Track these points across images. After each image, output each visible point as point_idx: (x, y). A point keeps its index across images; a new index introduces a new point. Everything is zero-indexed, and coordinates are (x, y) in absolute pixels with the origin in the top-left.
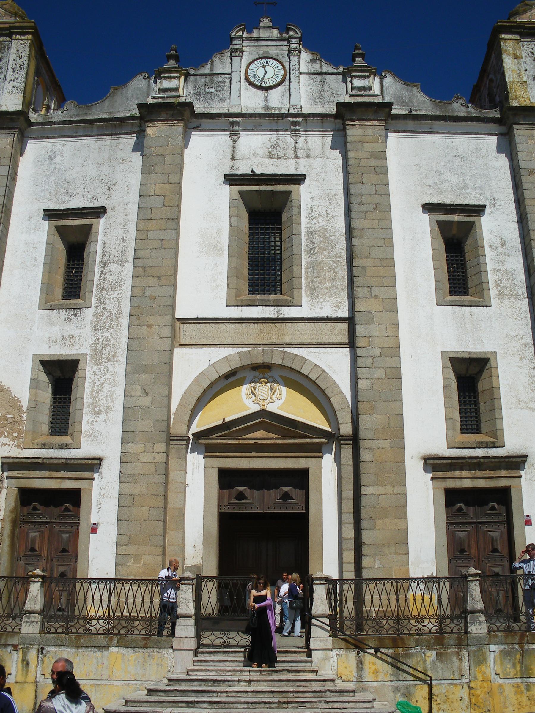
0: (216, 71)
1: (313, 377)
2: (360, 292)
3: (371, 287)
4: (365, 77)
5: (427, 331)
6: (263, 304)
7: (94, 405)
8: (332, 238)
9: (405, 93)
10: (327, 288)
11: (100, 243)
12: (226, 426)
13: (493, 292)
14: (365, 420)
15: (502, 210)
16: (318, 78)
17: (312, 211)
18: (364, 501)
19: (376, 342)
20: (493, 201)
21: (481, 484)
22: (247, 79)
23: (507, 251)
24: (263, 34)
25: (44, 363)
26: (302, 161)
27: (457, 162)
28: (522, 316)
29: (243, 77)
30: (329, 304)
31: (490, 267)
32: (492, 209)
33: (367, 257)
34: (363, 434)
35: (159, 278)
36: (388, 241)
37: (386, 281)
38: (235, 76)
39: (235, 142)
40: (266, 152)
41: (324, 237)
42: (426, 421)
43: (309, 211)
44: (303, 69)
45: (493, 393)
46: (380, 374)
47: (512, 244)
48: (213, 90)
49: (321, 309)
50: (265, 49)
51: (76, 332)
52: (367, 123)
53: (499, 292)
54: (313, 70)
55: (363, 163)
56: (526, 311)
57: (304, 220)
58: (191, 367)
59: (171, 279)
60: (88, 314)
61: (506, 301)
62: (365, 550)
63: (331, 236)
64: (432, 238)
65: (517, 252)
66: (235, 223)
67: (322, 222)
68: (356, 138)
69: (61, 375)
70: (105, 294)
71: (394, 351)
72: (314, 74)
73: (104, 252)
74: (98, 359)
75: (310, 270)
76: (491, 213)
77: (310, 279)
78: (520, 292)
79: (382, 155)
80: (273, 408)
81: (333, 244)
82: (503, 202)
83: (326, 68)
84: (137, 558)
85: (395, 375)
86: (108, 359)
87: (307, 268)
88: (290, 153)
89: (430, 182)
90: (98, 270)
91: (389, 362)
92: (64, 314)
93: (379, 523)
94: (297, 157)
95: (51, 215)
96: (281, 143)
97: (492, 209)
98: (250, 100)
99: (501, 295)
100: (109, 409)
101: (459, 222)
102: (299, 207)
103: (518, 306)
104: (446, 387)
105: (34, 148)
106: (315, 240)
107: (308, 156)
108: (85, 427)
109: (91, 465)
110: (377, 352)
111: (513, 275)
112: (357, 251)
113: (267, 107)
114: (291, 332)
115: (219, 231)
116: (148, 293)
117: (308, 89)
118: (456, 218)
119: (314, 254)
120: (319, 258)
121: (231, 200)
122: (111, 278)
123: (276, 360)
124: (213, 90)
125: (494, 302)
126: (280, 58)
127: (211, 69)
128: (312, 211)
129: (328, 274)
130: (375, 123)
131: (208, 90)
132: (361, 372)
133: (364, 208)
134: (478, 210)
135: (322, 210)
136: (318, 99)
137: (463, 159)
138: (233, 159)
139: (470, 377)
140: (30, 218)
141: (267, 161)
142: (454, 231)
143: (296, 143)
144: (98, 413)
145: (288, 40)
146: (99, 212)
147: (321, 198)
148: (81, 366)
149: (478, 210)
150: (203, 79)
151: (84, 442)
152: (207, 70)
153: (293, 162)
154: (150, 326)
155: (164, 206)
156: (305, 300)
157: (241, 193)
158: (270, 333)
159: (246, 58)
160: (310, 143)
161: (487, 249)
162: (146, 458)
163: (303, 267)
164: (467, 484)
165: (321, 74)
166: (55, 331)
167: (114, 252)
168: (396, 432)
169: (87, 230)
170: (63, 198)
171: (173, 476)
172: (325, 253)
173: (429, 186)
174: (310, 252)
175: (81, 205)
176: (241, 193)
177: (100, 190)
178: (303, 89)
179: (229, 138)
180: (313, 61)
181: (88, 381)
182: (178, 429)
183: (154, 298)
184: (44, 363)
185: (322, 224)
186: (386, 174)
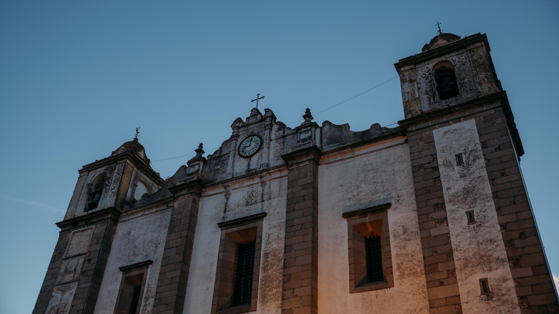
0: (223, 154)
3: (293, 289)
4: (308, 131)
8: (280, 255)
9: (337, 134)
10: (273, 294)
13: (396, 274)
15: (404, 204)
16: (281, 140)
17: (269, 238)
20: (397, 198)
22: (239, 154)
23: (407, 237)
26: (265, 203)
27: (371, 174)
28: (420, 290)
29: (237, 153)
30: (273, 306)
31: (393, 254)
32: (397, 205)
33: (293, 267)
35: (167, 305)
38: (231, 155)
39: (227, 199)
40: (245, 201)
41: (274, 255)
43: (267, 238)
44: (273, 136)
47: (412, 230)
48: (219, 167)
49: (268, 311)
52: (301, 165)
53: (401, 273)
54: (279, 135)
56: (423, 286)
57: (263, 245)
61: (406, 280)
63: (279, 254)
64: (349, 239)
65: (417, 236)
66: (221, 258)
67: (274, 245)
72: (279, 139)
73: (148, 290)
75: (264, 282)
76: (396, 208)
77: (263, 290)
78: (418, 270)
82: (405, 197)
87: (262, 281)
88: (260, 198)
89: (349, 196)
90: (143, 303)
95: (124, 269)
96: (254, 193)
97: (397, 205)
99: (402, 275)
102: (261, 237)
103: (417, 282)
105: (121, 229)
106: (269, 259)
111: (412, 256)
115: (212, 264)
117: (275, 150)
119: (267, 270)
120: (270, 272)
121: (221, 241)
125: (396, 283)
127: (220, 153)
128: (269, 238)
129: (275, 283)
130: (307, 163)
131: (216, 168)
133: (294, 229)
135: (274, 236)
137: (375, 170)
138: (225, 211)
141: (244, 208)
143: (263, 191)
147: (275, 227)
155: (177, 254)
156: (259, 305)
159: (240, 140)
160: (272, 188)
161: (392, 239)
163: (260, 281)
170: (132, 258)
172: (274, 268)
173: (349, 199)
174: (265, 270)
175: (141, 261)
176: (227, 234)
177: (151, 249)
178: (272, 151)
179: (224, 198)
185: (274, 246)
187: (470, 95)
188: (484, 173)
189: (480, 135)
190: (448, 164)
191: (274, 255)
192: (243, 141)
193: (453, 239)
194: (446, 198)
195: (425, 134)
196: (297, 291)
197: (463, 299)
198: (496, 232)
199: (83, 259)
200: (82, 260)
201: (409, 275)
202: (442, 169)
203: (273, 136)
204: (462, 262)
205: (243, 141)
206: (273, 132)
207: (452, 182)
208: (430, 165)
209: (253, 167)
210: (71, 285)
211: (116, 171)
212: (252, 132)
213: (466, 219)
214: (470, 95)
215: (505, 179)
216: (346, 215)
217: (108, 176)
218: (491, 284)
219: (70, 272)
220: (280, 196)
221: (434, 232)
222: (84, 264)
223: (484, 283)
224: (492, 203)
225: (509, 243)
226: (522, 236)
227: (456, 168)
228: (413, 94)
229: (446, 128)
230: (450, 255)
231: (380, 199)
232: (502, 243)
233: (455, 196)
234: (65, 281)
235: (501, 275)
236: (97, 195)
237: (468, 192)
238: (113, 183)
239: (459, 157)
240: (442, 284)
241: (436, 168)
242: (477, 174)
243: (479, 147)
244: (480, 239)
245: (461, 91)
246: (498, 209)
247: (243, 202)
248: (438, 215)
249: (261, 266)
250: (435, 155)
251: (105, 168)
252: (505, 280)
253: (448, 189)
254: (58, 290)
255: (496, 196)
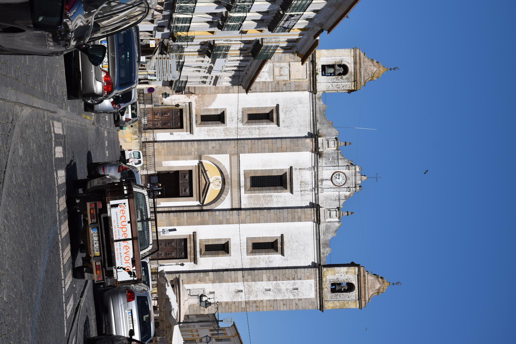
0: (340, 161)
1: (221, 198)
2: (248, 212)
5: (239, 234)
6: (245, 181)
7: (210, 130)
9: (332, 230)
11: (266, 126)
12: (205, 171)
13: (252, 257)
14: (206, 213)
18: (182, 213)
19: (231, 217)
21: (189, 250)
24: (358, 177)
25: (224, 112)
26: (300, 192)
34: (202, 213)
35: (251, 148)
36: (266, 221)
37: (252, 220)
39: (307, 169)
41: (270, 201)
42: (208, 232)
44: (341, 193)
45: (217, 255)
46: (221, 218)
48: (331, 160)
50: (351, 178)
51: (234, 122)
55: (296, 214)
57: (276, 194)
58: (224, 160)
59: (251, 151)
60: (241, 125)
61: (249, 261)
62: (167, 214)
67: (275, 200)
68: (306, 211)
69: (220, 118)
70: (248, 130)
71: (228, 222)
73: (263, 128)
74: (225, 130)
79: (300, 220)
80: (211, 186)
81: (267, 204)
83: (342, 202)
84: (163, 149)
85: (221, 223)
86: (225, 133)
88: (303, 189)
90: (256, 126)
91: (225, 221)
92: (240, 117)
93: (176, 218)
94: (301, 191)
95: (278, 106)
98: (326, 173)
99: (251, 259)
100: (209, 135)
101: (277, 247)
102: (281, 192)
104: (219, 239)
107: (301, 195)
108: (203, 128)
109: (191, 132)
110: (228, 217)
112: (262, 211)
113: (322, 180)
114: (235, 190)
116: (246, 146)
118: (279, 246)
120: (262, 199)
121: (283, 170)
122: (253, 131)
123: (226, 186)
124: (331, 160)
125: (249, 256)
126: (346, 184)
127: (341, 159)
130: (313, 218)
132: (221, 212)
133: (278, 214)
134: (282, 254)
135: (280, 200)
136: (327, 198)
138: (300, 169)
139: (223, 248)
140: (277, 99)
142: (276, 245)
144: (208, 132)
145: (355, 187)
146: (278, 124)
148: (223, 125)
149: (282, 254)
150: (336, 156)
151: (198, 128)
152: (340, 157)
153: (299, 190)
154: (235, 147)
156: (247, 195)
157: (286, 173)
158: (235, 184)
159: (346, 171)
161: (268, 256)
162: (193, 149)
164: (188, 245)
165: (339, 200)
166: (235, 115)
167: (263, 131)
168: (203, 223)
169: (272, 120)
171: (189, 157)
174: (264, 196)
178: (332, 193)
180: (346, 196)
181: (218, 127)
182: (203, 157)
183: (244, 147)
184: (224, 112)
186: (292, 221)
187: (329, 297)
188: (286, 298)
189: (305, 299)
190: (294, 284)
191: (270, 201)
192: (344, 174)
193: (260, 282)
194: (279, 282)
195: (313, 276)
196: (248, 217)
197: (236, 283)
198: (260, 298)
199: (287, 79)
200: (286, 78)
201: (251, 262)
202: (293, 281)
203: (341, 193)
204: (250, 284)
205: (344, 174)
206: (345, 193)
207: (286, 285)
208: (296, 277)
209: (324, 182)
210: (272, 76)
211: (346, 83)
212: (349, 179)
213: (268, 288)
214: (329, 297)
215: (282, 305)
216: (282, 236)
217: (344, 77)
218: (241, 293)
219: (280, 71)
220: (302, 201)
221: (265, 276)
222: (284, 81)
223: (242, 291)
224: (272, 299)
225: (255, 302)
226: (257, 306)
227: (292, 287)
228: (338, 273)
229: (313, 285)
230: (254, 281)
231: (285, 253)
232: (255, 299)
233: (279, 285)
234: (275, 69)
235: (242, 298)
236: (332, 71)
237: (280, 291)
238: (337, 84)
239: (297, 289)
240: (243, 277)
241: (294, 279)
242: (286, 295)
243: (300, 298)
244: (258, 292)
245: (333, 294)
246: (269, 300)
247: (303, 179)
248: (272, 278)
249: (266, 194)
250: (301, 279)
251: (353, 71)
252: (241, 298)
253: (283, 283)
254: (270, 67)
255: (275, 300)
